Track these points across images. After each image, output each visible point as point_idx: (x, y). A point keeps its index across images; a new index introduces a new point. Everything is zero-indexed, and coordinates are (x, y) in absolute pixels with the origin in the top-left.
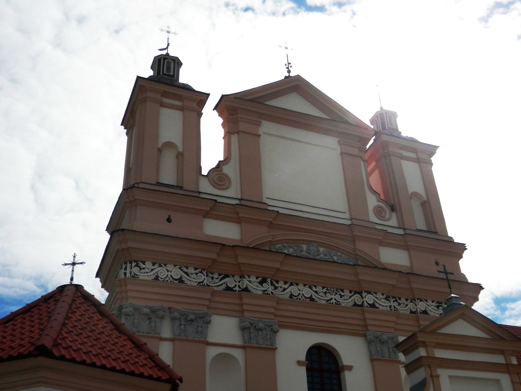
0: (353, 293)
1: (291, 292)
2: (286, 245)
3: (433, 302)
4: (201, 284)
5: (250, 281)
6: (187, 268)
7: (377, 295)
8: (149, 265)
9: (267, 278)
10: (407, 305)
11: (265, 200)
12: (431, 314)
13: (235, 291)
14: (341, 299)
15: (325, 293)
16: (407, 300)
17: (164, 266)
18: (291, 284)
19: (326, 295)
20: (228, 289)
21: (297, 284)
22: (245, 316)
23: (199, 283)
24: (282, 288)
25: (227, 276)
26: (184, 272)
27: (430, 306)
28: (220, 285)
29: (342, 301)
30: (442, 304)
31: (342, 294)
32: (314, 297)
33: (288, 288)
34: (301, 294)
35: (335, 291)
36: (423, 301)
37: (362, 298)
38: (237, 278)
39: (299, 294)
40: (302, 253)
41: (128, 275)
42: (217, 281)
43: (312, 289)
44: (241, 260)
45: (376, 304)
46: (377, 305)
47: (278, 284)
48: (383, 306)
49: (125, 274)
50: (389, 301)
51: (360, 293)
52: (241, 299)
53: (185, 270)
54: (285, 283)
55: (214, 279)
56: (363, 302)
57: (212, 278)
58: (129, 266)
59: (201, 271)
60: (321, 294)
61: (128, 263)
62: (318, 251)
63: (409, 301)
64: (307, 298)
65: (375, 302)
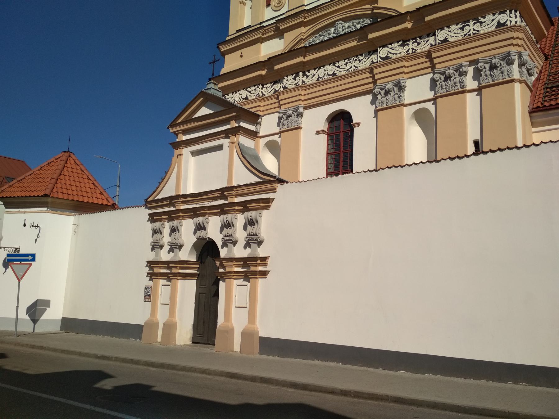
0: (371, 53)
1: (318, 76)
3: (457, 24)
4: (257, 96)
14: (360, 63)
23: (256, 95)
24: (312, 75)
27: (452, 31)
28: (271, 92)
30: (469, 22)
32: (336, 72)
34: (326, 74)
36: (444, 29)
39: (325, 74)
40: (330, 36)
43: (335, 65)
46: (390, 56)
47: (309, 72)
54: (315, 69)
55: (268, 88)
57: (267, 88)
64: (330, 75)
65: (389, 54)
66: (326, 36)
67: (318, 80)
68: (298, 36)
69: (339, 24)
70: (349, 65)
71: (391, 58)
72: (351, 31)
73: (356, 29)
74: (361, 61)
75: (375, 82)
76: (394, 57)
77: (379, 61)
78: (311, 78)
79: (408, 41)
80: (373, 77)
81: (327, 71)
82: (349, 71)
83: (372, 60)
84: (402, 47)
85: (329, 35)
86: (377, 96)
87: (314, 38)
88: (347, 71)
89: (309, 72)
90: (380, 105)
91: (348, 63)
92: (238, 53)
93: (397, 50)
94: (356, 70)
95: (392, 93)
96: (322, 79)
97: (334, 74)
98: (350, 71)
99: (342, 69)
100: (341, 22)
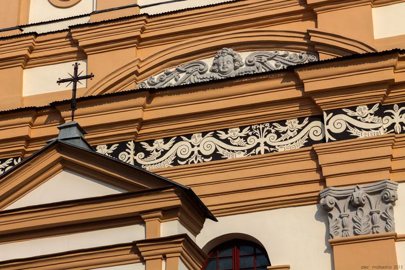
0: (305, 122)
1: (176, 155)
7: (356, 111)
9: (127, 142)
14: (279, 139)
18: (179, 139)
19: (246, 141)
21: (189, 136)
24: (160, 152)
31: (282, 129)
32: (221, 151)
33: (171, 148)
34: (196, 153)
35: (268, 128)
39: (193, 153)
40: (204, 76)
43: (218, 138)
46: (354, 132)
47: (152, 145)
48: (368, 130)
54: (166, 140)
59: (11, 162)
65: (349, 127)
66: (194, 74)
67: (175, 163)
68: (126, 66)
69: (226, 54)
70: (253, 141)
71: (357, 137)
72: (254, 71)
73: (268, 70)
74: (283, 135)
75: (322, 181)
76: (363, 135)
77: (327, 140)
78: (157, 158)
79: (391, 107)
80: (319, 169)
81: (198, 146)
82: (253, 152)
83: (308, 136)
84: (380, 118)
85: (200, 73)
86: (330, 212)
87: (163, 76)
88: (248, 153)
89: (152, 145)
90: (338, 233)
91: (250, 136)
93: (367, 122)
94: (271, 152)
95: (366, 209)
96: (185, 162)
97: (216, 156)
98: (257, 153)
99: (236, 146)
100: (230, 50)
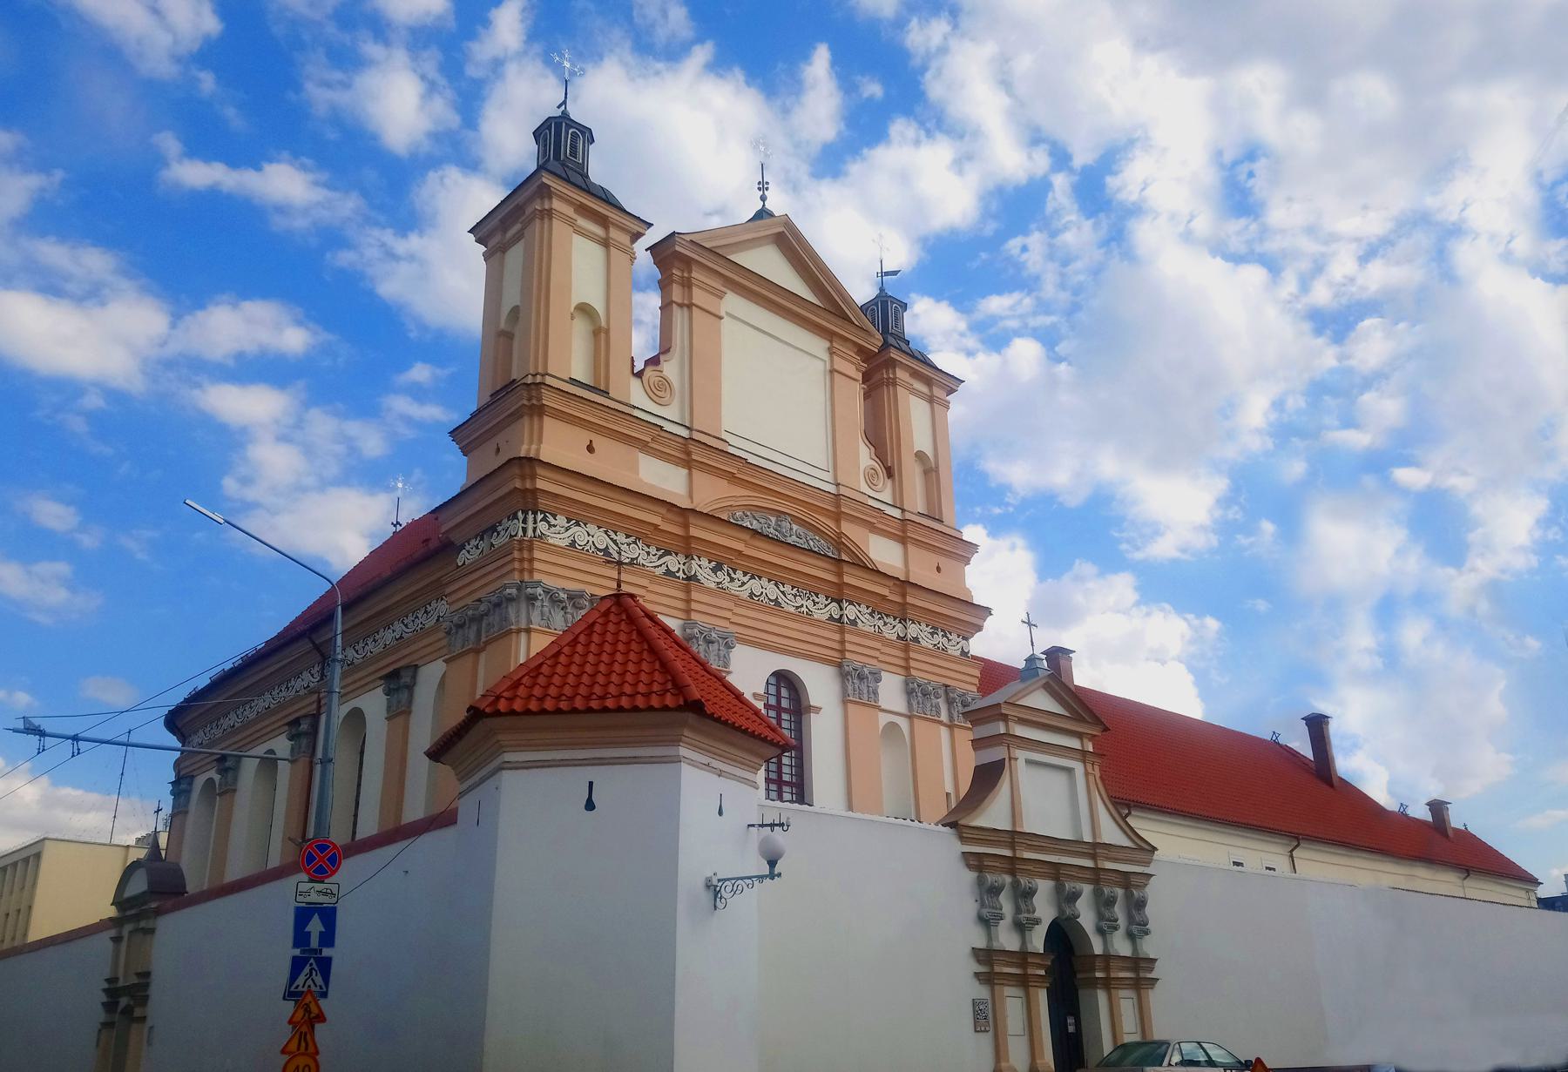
0: (829, 601)
2: (749, 513)
3: (927, 626)
5: (699, 566)
6: (615, 533)
8: (561, 520)
10: (894, 627)
11: (724, 436)
12: (923, 643)
13: (679, 578)
15: (795, 596)
16: (895, 619)
17: (583, 526)
18: (752, 577)
20: (668, 573)
21: (760, 578)
22: (691, 620)
25: (667, 553)
26: (611, 539)
28: (658, 566)
29: (816, 611)
31: (817, 600)
32: (780, 600)
37: (841, 609)
38: (682, 558)
41: (530, 533)
42: (655, 559)
44: (694, 532)
45: (858, 620)
49: (524, 530)
50: (873, 617)
51: (839, 602)
52: (688, 591)
53: (613, 536)
54: (745, 574)
56: (841, 616)
57: (648, 553)
58: (530, 517)
60: (790, 597)
61: (530, 512)
62: (791, 529)
63: (897, 620)
92: (584, 436)
